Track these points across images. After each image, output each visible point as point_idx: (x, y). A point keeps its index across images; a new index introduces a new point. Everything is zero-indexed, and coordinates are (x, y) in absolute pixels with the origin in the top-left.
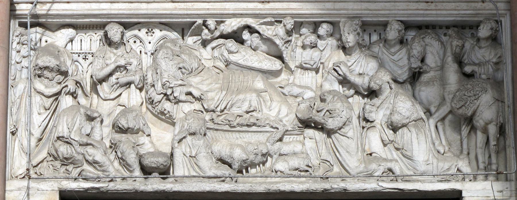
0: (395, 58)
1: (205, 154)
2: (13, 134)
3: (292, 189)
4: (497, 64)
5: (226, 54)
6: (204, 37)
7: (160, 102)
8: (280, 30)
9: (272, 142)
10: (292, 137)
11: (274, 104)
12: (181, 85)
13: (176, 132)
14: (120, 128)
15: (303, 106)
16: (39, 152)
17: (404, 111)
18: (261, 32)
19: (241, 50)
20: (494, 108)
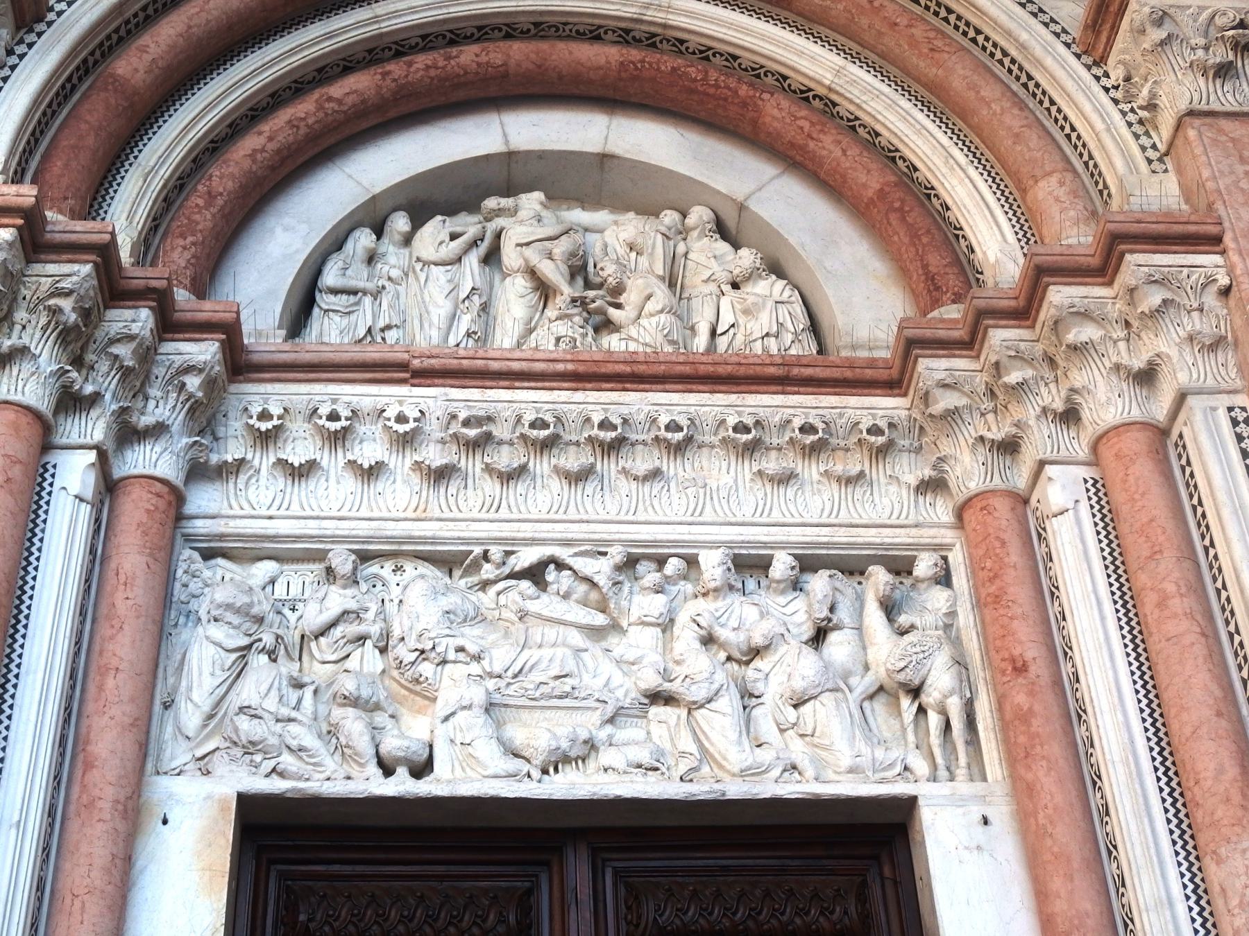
0: (788, 610)
2: (167, 706)
5: (518, 599)
7: (413, 663)
14: (345, 698)
16: (208, 737)
18: (575, 568)
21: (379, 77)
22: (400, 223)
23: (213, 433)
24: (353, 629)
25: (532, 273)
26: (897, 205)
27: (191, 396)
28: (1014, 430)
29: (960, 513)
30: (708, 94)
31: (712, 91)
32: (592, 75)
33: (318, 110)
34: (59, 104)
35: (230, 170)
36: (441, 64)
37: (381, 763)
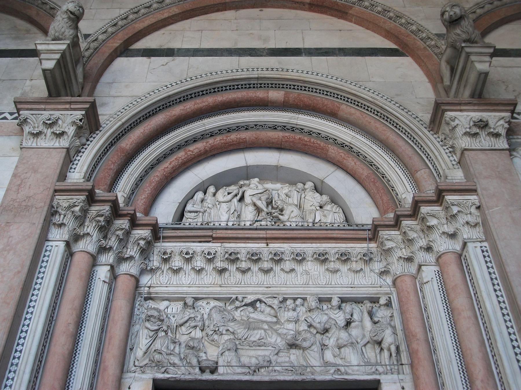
0: (337, 316)
1: (236, 361)
2: (131, 349)
3: (284, 379)
4: (391, 317)
5: (248, 313)
6: (236, 306)
7: (212, 335)
8: (276, 302)
9: (272, 355)
10: (284, 354)
11: (274, 336)
12: (223, 326)
13: (220, 350)
14: (189, 346)
15: (289, 337)
16: (144, 360)
17: (344, 337)
19: (256, 312)
20: (393, 336)
21: (205, 143)
22: (212, 189)
23: (149, 259)
24: (193, 324)
25: (255, 205)
26: (372, 180)
27: (141, 247)
28: (411, 254)
29: (394, 282)
30: (310, 146)
31: (312, 145)
32: (274, 141)
33: (185, 155)
34: (103, 156)
35: (157, 174)
36: (225, 139)
37: (201, 369)
